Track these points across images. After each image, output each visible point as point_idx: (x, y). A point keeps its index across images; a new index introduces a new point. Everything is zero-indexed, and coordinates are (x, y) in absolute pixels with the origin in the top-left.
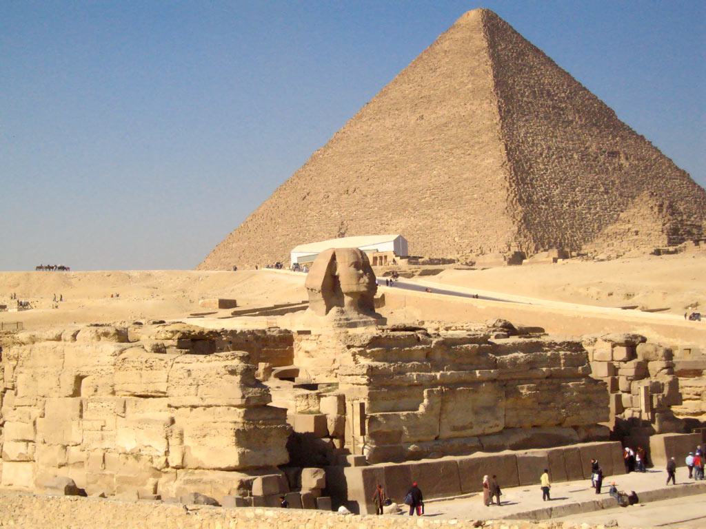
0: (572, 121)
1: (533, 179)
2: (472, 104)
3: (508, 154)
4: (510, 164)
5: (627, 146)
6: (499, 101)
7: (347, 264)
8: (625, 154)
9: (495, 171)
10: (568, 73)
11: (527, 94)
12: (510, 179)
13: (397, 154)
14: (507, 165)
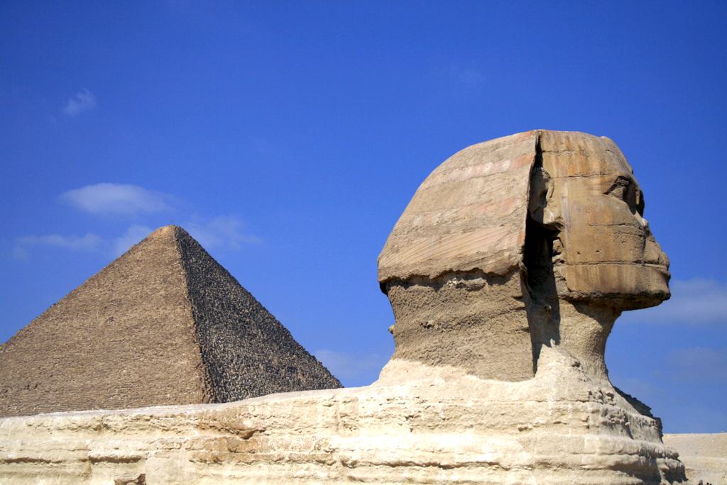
0: (255, 335)
1: (226, 383)
2: (165, 309)
3: (203, 356)
4: (204, 367)
5: (303, 364)
6: (192, 307)
7: (596, 181)
8: (302, 370)
9: (189, 373)
10: (250, 293)
11: (216, 305)
12: (206, 380)
13: (84, 353)
14: (201, 367)
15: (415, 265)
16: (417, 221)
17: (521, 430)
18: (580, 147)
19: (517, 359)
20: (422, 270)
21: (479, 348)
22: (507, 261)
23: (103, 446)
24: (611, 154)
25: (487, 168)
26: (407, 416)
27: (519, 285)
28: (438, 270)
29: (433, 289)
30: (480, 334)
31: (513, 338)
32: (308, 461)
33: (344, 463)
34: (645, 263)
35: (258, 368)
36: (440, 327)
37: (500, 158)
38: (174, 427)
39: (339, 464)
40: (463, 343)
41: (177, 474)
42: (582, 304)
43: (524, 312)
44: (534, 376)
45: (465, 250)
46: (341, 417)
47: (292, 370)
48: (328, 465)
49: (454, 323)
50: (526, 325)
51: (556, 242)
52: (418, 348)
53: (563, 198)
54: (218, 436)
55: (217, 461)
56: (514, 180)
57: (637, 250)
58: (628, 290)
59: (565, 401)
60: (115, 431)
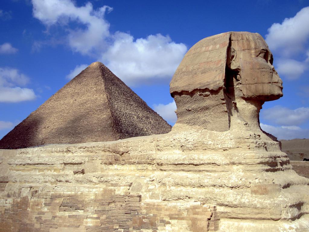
1: (122, 124)
3: (112, 114)
4: (113, 118)
7: (253, 51)
9: (107, 120)
10: (129, 88)
15: (183, 87)
17: (224, 150)
18: (246, 38)
19: (223, 123)
20: (186, 89)
21: (208, 118)
22: (218, 85)
24: (259, 40)
26: (181, 146)
27: (223, 94)
28: (192, 89)
29: (190, 96)
30: (209, 113)
31: (221, 115)
32: (145, 164)
33: (158, 164)
34: (273, 83)
35: (134, 117)
36: (194, 111)
37: (215, 44)
38: (94, 151)
39: (156, 164)
40: (202, 116)
41: (96, 169)
42: (248, 99)
43: (225, 105)
44: (229, 129)
45: (202, 81)
46: (157, 146)
47: (147, 118)
48: (152, 165)
49: (199, 109)
50: (226, 110)
51: (238, 76)
52: (185, 119)
53: (240, 58)
54: (111, 154)
56: (221, 52)
57: (269, 78)
58: (266, 94)
59: (241, 139)
60: (72, 153)
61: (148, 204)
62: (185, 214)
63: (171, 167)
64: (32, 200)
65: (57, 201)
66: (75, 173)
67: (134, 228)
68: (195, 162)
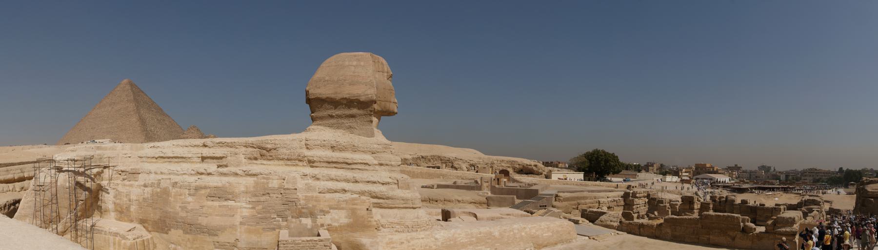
16: (327, 78)
21: (354, 125)
23: (206, 152)
25: (355, 63)
40: (347, 122)
55: (256, 159)
61: (306, 196)
62: (344, 205)
63: (325, 165)
64: (173, 191)
65: (203, 192)
66: (219, 166)
67: (292, 217)
68: (349, 161)
